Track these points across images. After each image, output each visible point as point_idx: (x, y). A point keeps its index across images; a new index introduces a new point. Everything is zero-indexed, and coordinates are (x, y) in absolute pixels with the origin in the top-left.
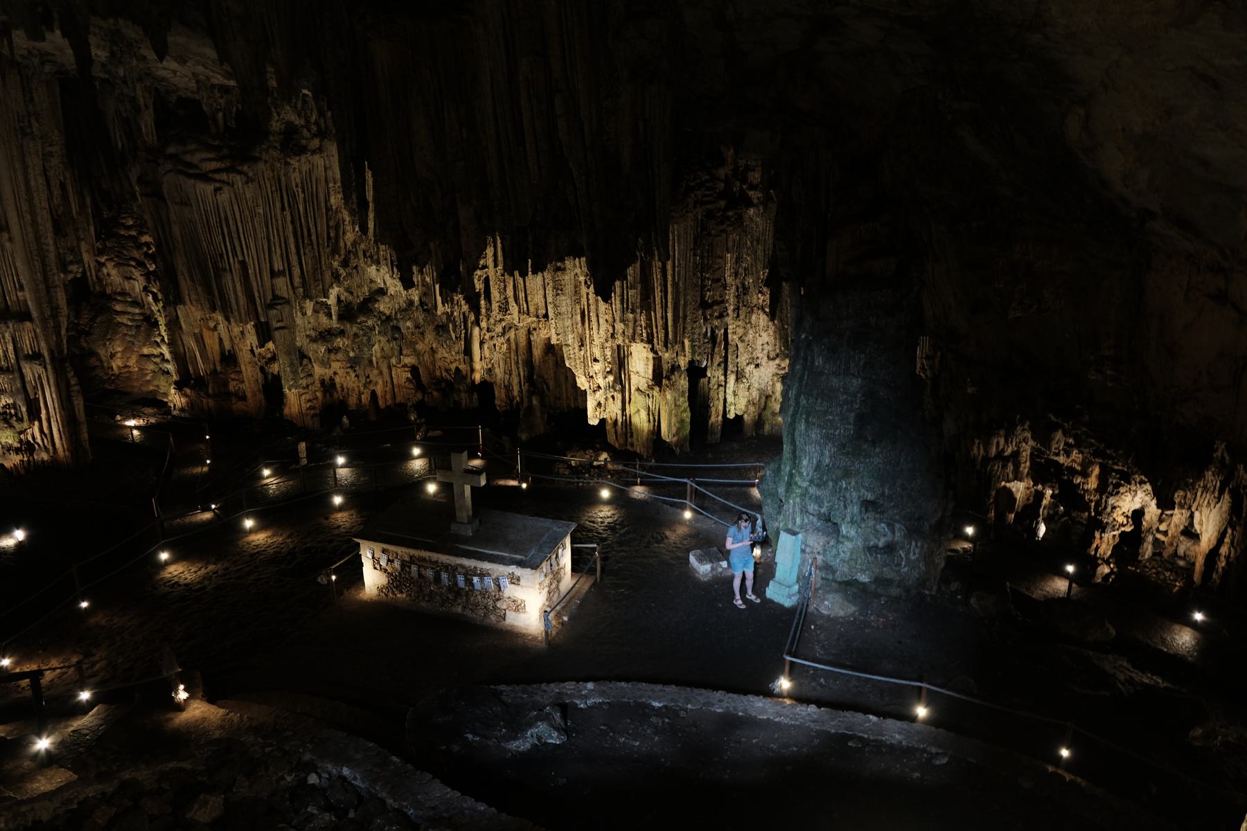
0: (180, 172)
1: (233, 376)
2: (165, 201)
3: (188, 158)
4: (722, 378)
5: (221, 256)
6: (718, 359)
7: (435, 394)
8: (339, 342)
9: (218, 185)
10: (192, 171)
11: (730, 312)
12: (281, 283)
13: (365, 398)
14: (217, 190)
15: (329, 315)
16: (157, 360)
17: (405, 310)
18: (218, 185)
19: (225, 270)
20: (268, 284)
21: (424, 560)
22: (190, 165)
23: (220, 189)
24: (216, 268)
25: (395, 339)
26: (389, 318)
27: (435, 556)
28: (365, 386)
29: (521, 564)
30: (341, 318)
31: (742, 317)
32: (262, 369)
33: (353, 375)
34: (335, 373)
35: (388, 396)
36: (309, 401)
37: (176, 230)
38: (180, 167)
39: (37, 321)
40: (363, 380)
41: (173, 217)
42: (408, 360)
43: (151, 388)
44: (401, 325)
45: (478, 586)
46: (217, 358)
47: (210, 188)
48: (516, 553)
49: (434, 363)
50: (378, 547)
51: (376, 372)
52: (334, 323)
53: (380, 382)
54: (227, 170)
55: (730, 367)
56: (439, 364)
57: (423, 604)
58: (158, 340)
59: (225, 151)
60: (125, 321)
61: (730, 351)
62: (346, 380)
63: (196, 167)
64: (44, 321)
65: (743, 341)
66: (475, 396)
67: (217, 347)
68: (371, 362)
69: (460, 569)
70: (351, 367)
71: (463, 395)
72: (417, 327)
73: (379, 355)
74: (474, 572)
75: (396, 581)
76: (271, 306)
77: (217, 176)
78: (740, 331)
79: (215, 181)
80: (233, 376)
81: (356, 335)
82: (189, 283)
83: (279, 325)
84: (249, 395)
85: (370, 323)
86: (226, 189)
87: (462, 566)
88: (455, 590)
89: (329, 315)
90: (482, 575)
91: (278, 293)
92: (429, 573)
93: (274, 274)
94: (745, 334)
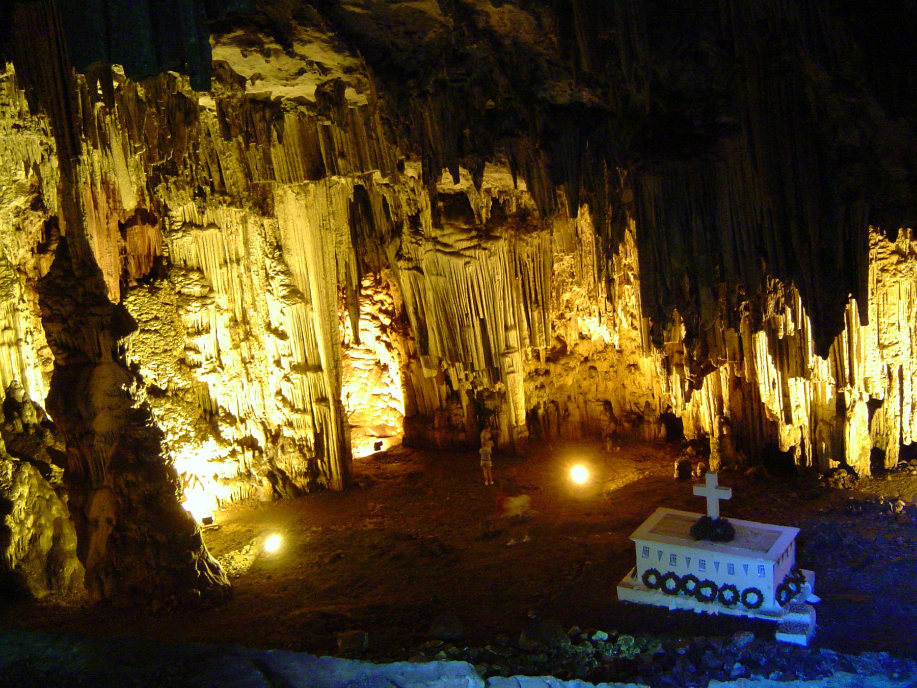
0: (438, 251)
2: (422, 273)
3: (445, 240)
5: (467, 315)
9: (467, 259)
10: (447, 250)
14: (465, 264)
18: (467, 259)
19: (468, 326)
22: (446, 245)
23: (469, 263)
37: (430, 295)
38: (438, 247)
39: (325, 371)
41: (428, 285)
47: (461, 262)
54: (474, 247)
59: (474, 233)
63: (451, 246)
64: (330, 372)
77: (467, 253)
79: (466, 256)
86: (473, 261)
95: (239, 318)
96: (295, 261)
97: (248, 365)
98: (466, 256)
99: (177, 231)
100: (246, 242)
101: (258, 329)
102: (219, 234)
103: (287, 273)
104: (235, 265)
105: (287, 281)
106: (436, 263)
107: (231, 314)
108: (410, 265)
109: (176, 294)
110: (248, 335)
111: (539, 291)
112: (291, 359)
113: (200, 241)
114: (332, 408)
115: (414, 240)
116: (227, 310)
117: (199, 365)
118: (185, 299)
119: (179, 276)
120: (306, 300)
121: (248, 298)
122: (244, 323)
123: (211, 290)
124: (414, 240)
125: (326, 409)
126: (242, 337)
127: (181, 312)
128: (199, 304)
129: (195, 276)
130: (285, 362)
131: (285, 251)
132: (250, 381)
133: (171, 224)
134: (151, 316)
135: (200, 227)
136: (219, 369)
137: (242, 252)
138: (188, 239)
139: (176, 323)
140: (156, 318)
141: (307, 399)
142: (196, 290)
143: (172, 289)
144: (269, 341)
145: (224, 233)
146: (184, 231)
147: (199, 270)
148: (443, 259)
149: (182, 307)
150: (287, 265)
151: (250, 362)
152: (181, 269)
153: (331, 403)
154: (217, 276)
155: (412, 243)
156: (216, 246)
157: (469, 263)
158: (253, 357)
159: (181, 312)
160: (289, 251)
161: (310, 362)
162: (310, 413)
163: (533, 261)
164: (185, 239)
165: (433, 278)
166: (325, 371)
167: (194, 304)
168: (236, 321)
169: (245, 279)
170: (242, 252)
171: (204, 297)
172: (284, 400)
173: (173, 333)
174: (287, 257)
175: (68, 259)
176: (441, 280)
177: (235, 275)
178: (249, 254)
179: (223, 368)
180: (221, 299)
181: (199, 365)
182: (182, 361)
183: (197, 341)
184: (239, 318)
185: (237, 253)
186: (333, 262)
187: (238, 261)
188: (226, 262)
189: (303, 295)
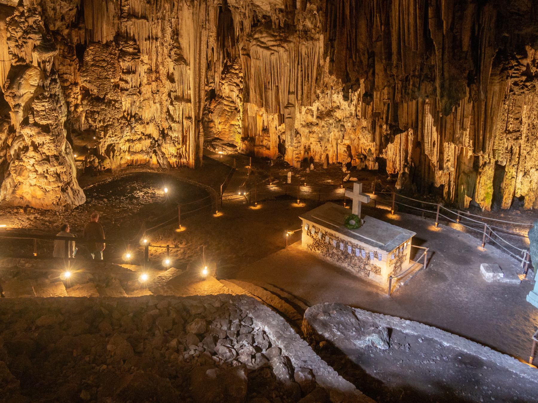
1: (266, 138)
4: (515, 173)
5: (269, 83)
6: (513, 163)
7: (357, 160)
8: (315, 129)
11: (523, 137)
12: (292, 97)
13: (323, 157)
15: (313, 116)
16: (237, 127)
17: (349, 118)
20: (286, 98)
21: (332, 235)
24: (266, 88)
25: (342, 131)
26: (340, 120)
27: (338, 234)
28: (324, 151)
29: (381, 247)
30: (318, 117)
31: (530, 141)
32: (279, 137)
33: (319, 145)
34: (311, 143)
35: (334, 158)
36: (297, 154)
39: (192, 103)
40: (323, 148)
42: (347, 142)
43: (232, 139)
44: (345, 124)
45: (358, 254)
46: (261, 129)
48: (380, 241)
49: (358, 145)
50: (311, 224)
51: (330, 145)
52: (314, 120)
53: (331, 150)
55: (520, 168)
56: (361, 145)
57: (328, 258)
58: (239, 118)
60: (227, 109)
61: (521, 159)
62: (316, 148)
64: (195, 103)
65: (529, 155)
66: (377, 164)
67: (261, 124)
68: (328, 140)
69: (349, 244)
70: (319, 141)
71: (371, 163)
72: (353, 126)
73: (333, 137)
74: (356, 246)
75: (317, 244)
76: (286, 107)
78: (528, 149)
80: (266, 138)
81: (323, 126)
82: (254, 93)
83: (289, 116)
84: (271, 147)
85: (331, 121)
87: (351, 242)
88: (346, 255)
89: (313, 116)
90: (361, 249)
91: (290, 102)
92: (334, 243)
93: (289, 93)
94: (531, 151)
95: (154, 68)
96: (184, 42)
97: (155, 95)
98: (272, 50)
99: (125, 18)
100: (163, 30)
101: (164, 78)
102: (147, 23)
103: (179, 48)
104: (154, 41)
105: (178, 52)
106: (256, 52)
107: (148, 66)
108: (245, 53)
109: (119, 50)
110: (157, 79)
111: (310, 75)
112: (175, 94)
113: (136, 25)
114: (193, 123)
115: (248, 39)
116: (146, 64)
117: (127, 90)
118: (123, 54)
119: (122, 42)
120: (187, 64)
121: (160, 59)
122: (156, 72)
123: (139, 52)
124: (248, 39)
125: (190, 123)
126: (153, 79)
127: (120, 60)
128: (131, 58)
129: (131, 43)
130: (172, 94)
131: (180, 37)
132: (155, 103)
133: (121, 14)
134: (100, 59)
135: (137, 17)
136: (138, 94)
137: (160, 35)
138: (130, 23)
139: (116, 65)
140: (104, 60)
141: (181, 116)
142: (131, 50)
143: (117, 47)
144: (168, 83)
145: (150, 22)
146: (128, 18)
147: (135, 40)
148: (260, 50)
149: (121, 57)
150: (179, 44)
151: (156, 93)
152: (124, 38)
153: (193, 120)
154: (144, 45)
155: (247, 40)
156: (144, 29)
157: (273, 53)
158: (158, 91)
159: (120, 60)
160: (182, 36)
161: (186, 97)
162: (181, 124)
163: (308, 57)
164: (128, 23)
165: (254, 60)
166: (192, 103)
167: (128, 57)
168: (151, 70)
169: (159, 49)
170: (160, 35)
171: (133, 54)
172: (170, 115)
173: (112, 70)
174: (180, 39)
175: (23, 6)
176: (258, 61)
177: (154, 46)
178: (163, 36)
179: (140, 94)
180: (145, 58)
181: (127, 90)
182: (117, 86)
183: (128, 78)
184: (154, 68)
185: (157, 35)
186: (205, 46)
187: (157, 39)
188: (149, 37)
189: (186, 61)
